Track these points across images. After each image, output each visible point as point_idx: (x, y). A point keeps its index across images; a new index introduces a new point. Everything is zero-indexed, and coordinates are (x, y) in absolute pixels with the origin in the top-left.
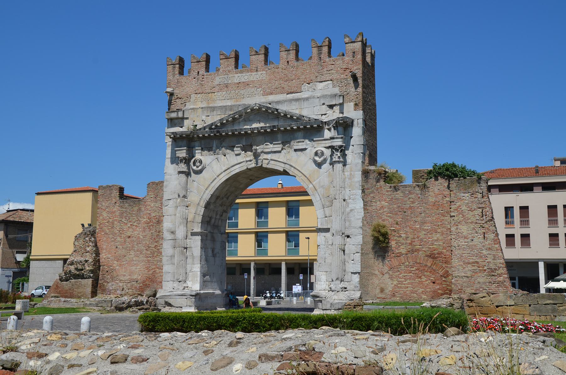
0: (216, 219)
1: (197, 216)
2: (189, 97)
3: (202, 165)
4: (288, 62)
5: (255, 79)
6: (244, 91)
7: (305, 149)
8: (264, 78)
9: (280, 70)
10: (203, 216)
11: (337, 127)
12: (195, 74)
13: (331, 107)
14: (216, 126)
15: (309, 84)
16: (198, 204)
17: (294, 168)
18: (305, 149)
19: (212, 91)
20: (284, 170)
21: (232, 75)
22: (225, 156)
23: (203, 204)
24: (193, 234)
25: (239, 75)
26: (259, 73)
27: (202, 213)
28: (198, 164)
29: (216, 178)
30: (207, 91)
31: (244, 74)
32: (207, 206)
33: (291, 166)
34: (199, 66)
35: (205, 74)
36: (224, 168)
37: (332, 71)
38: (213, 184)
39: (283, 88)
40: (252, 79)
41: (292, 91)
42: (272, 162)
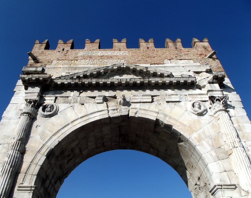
0: (50, 183)
1: (33, 166)
2: (50, 62)
3: (54, 110)
4: (148, 48)
5: (118, 54)
6: (108, 60)
7: (179, 102)
8: (126, 55)
9: (142, 51)
10: (42, 167)
11: (213, 83)
12: (61, 49)
13: (198, 73)
14: (79, 77)
15: (170, 60)
16: (39, 151)
17: (170, 118)
18: (179, 102)
19: (75, 59)
20: (156, 119)
21: (96, 52)
22: (83, 104)
23: (45, 151)
24: (22, 189)
25: (103, 52)
26: (122, 52)
27: (41, 163)
28: (48, 109)
29: (68, 124)
30: (71, 59)
31: (108, 52)
32: (51, 155)
33: (166, 116)
34: (65, 46)
35: (70, 50)
36: (80, 116)
37: (190, 55)
38: (63, 131)
39: (146, 61)
40: (115, 54)
41: (155, 63)
42: (142, 112)
